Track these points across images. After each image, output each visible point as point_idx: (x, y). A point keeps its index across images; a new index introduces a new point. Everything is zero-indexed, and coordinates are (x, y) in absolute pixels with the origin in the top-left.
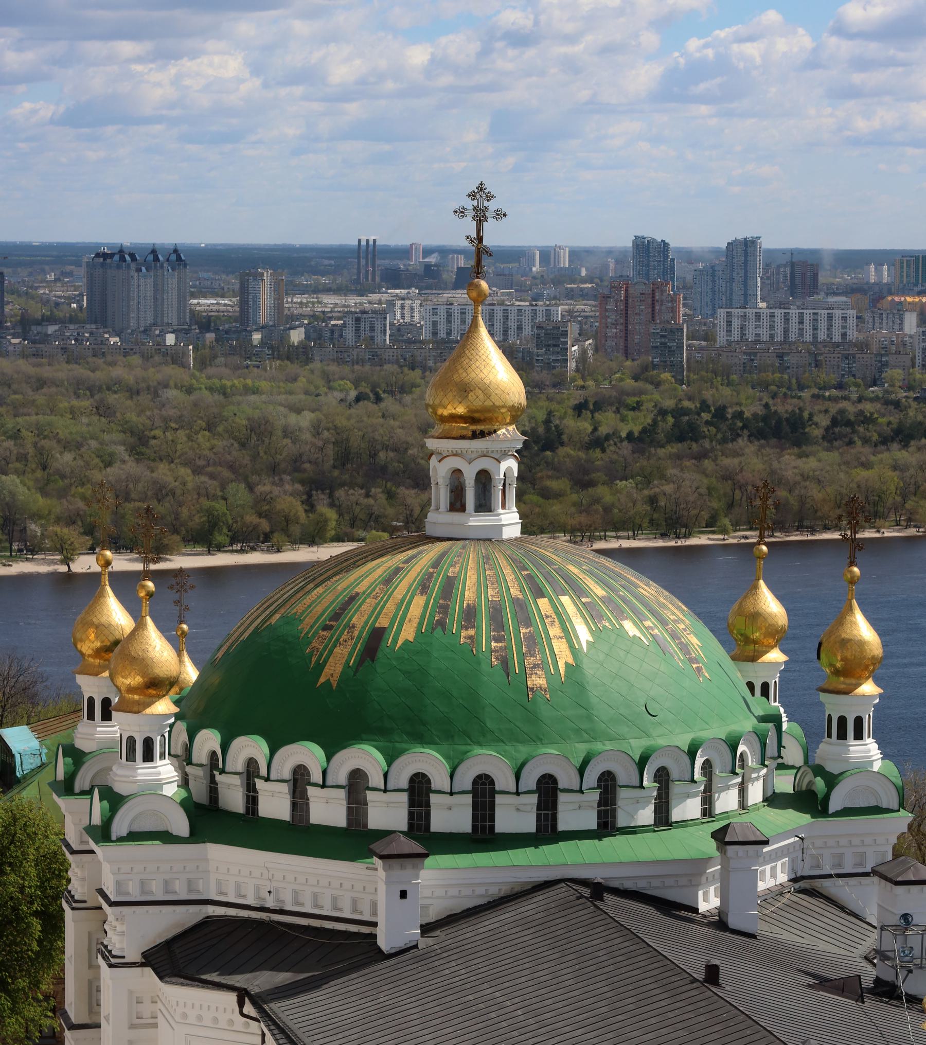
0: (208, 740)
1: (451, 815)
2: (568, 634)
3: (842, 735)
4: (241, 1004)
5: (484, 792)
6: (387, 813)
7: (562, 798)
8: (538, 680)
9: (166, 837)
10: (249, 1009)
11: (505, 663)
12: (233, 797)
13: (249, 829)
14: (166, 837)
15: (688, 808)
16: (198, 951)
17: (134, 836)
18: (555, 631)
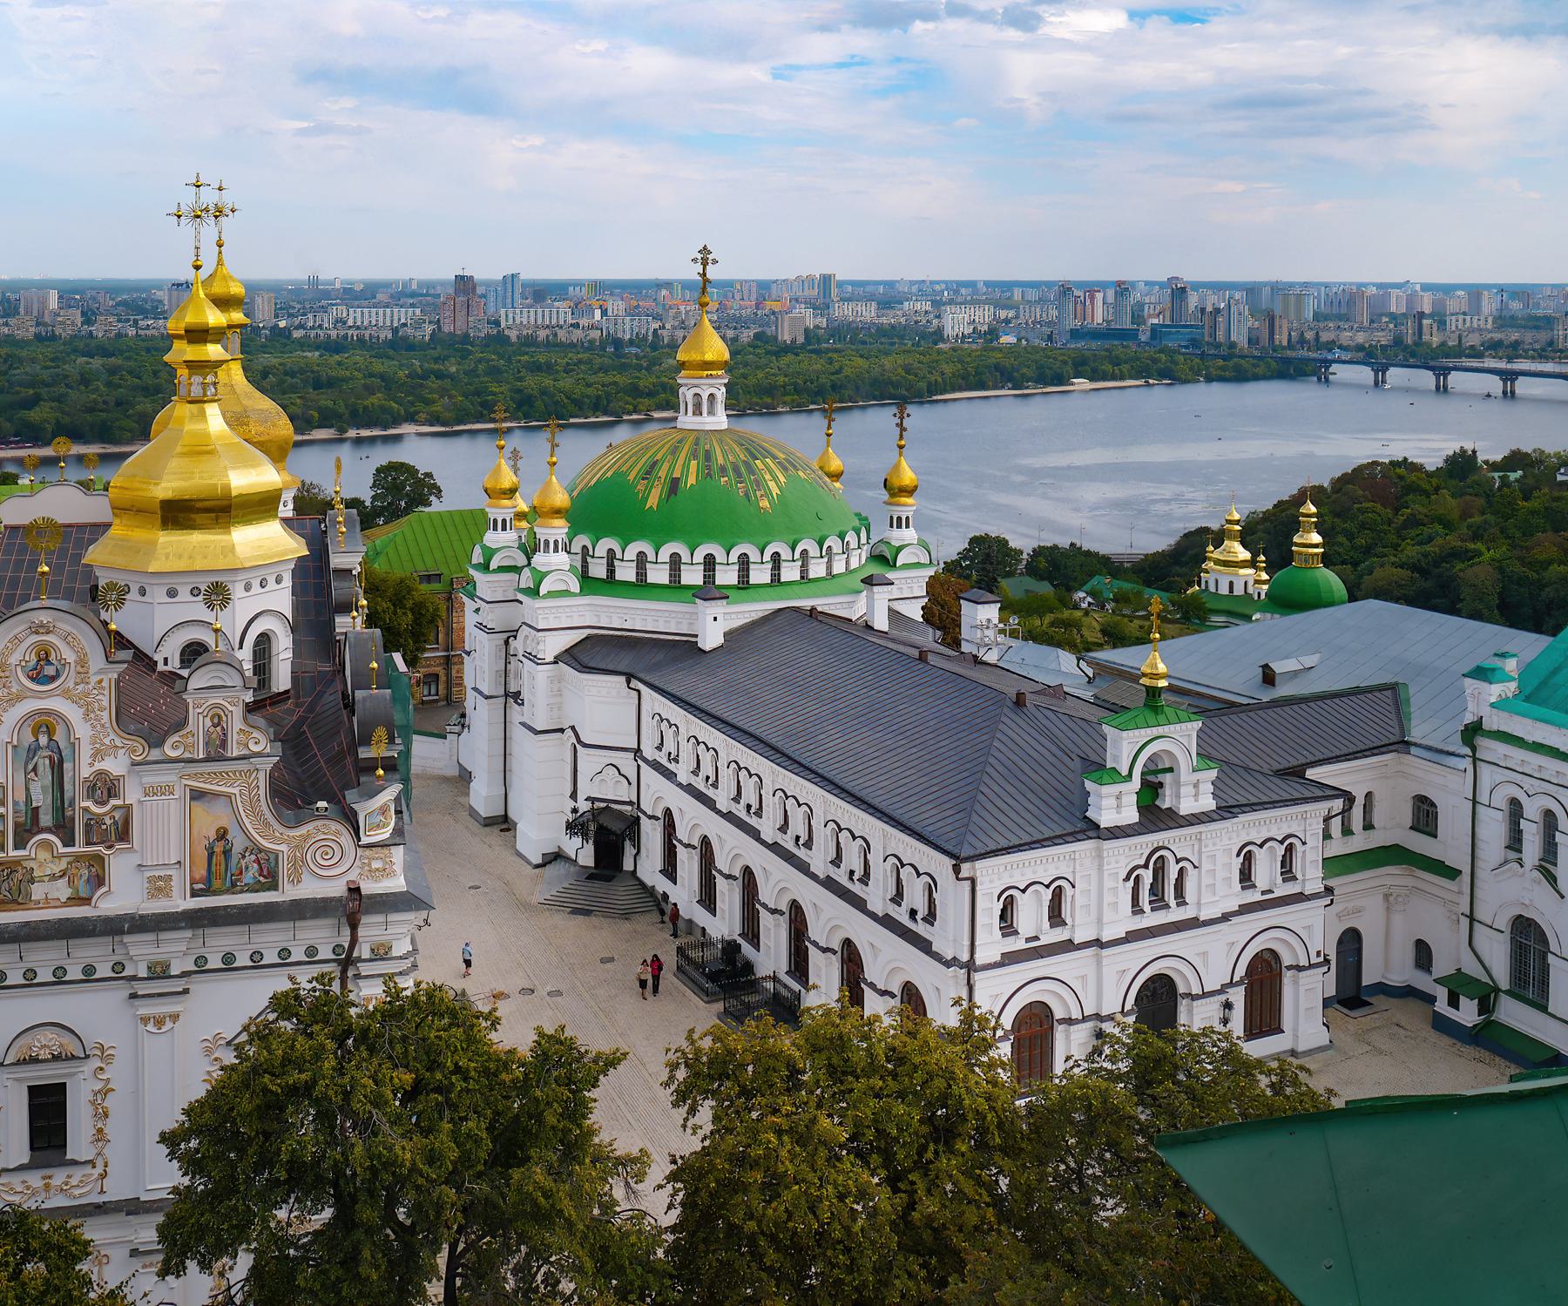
0: (582, 540)
1: (727, 576)
2: (775, 479)
3: (899, 526)
4: (628, 682)
5: (744, 562)
6: (693, 576)
7: (783, 564)
8: (765, 503)
9: (566, 593)
10: (635, 683)
11: (747, 495)
12: (598, 570)
13: (610, 584)
14: (566, 593)
15: (839, 567)
16: (592, 653)
17: (552, 594)
18: (768, 477)
